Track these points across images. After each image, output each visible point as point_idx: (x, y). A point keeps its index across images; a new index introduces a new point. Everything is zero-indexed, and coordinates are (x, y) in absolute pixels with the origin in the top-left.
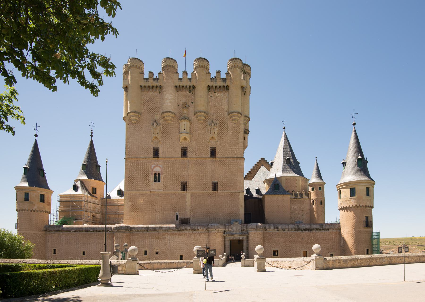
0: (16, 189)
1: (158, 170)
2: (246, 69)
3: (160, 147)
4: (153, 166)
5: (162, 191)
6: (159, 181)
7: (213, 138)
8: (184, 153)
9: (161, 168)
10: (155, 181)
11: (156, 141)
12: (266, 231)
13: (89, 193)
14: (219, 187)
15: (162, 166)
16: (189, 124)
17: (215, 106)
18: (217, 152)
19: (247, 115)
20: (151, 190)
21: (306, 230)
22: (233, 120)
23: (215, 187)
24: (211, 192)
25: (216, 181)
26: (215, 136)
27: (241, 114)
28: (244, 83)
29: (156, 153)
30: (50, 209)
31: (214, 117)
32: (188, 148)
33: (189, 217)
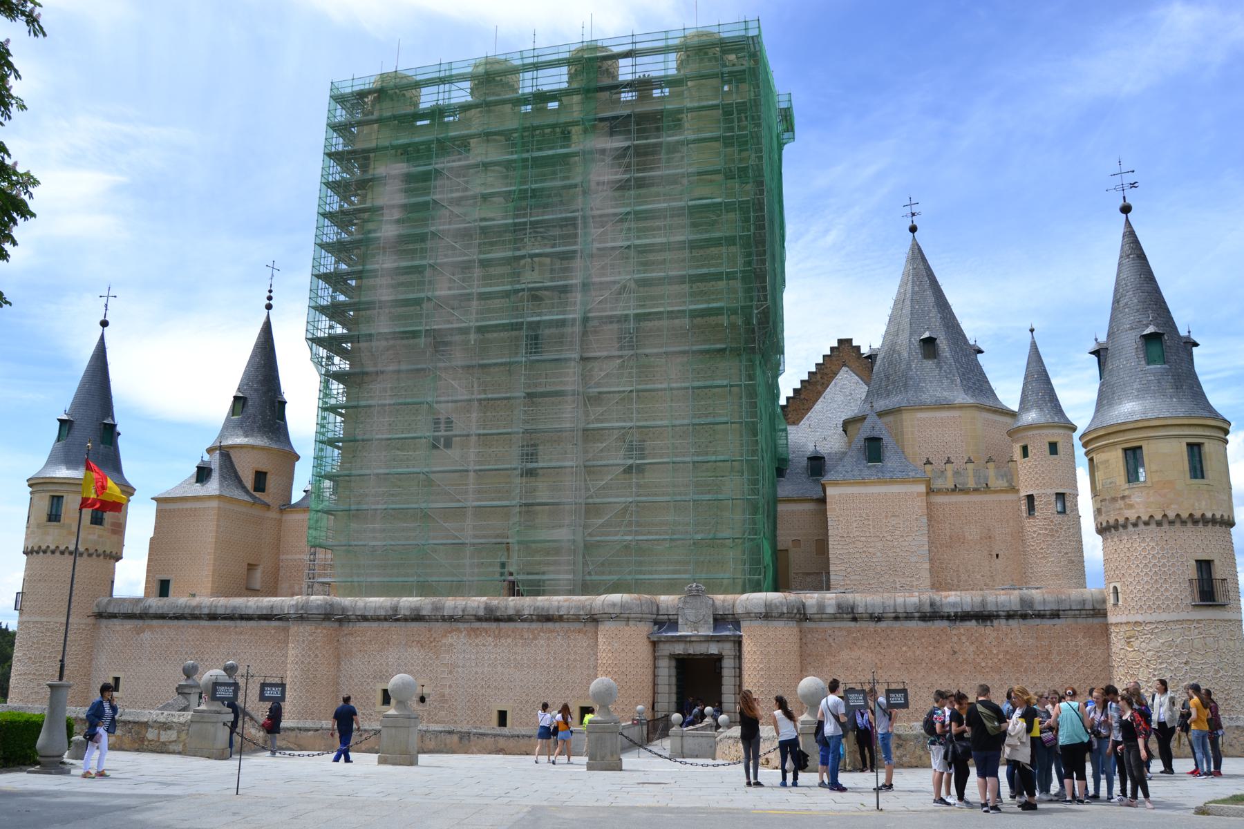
0: (30, 486)
13: (247, 492)
21: (964, 617)
30: (121, 544)
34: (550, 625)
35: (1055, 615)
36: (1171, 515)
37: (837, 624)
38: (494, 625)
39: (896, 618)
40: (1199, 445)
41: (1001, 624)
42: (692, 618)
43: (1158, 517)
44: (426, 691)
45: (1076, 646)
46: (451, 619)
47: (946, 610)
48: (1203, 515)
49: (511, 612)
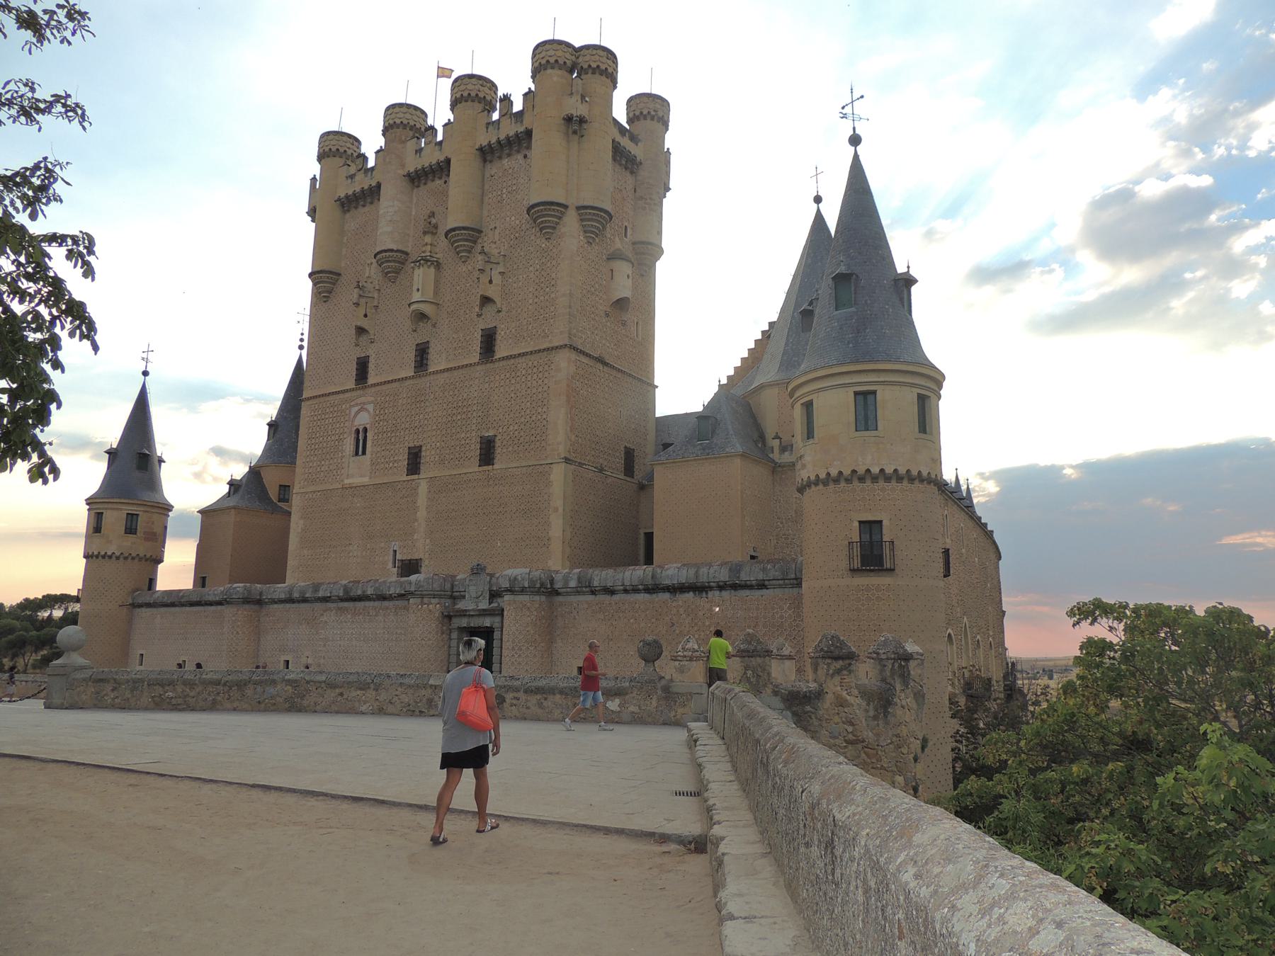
1: (363, 419)
3: (371, 352)
4: (355, 409)
5: (366, 480)
6: (364, 453)
7: (486, 300)
10: (357, 454)
11: (364, 338)
12: (560, 598)
14: (498, 451)
15: (370, 407)
16: (432, 270)
18: (498, 337)
20: (346, 481)
22: (541, 230)
23: (487, 453)
24: (477, 469)
25: (491, 434)
26: (489, 294)
27: (566, 207)
31: (497, 231)
32: (431, 344)
33: (421, 556)
34: (386, 603)
35: (762, 585)
36: (834, 473)
37: (581, 598)
38: (351, 604)
39: (626, 591)
40: (874, 393)
41: (714, 595)
42: (474, 595)
43: (823, 476)
44: (310, 661)
45: (782, 617)
46: (325, 600)
47: (667, 582)
48: (868, 471)
49: (359, 592)
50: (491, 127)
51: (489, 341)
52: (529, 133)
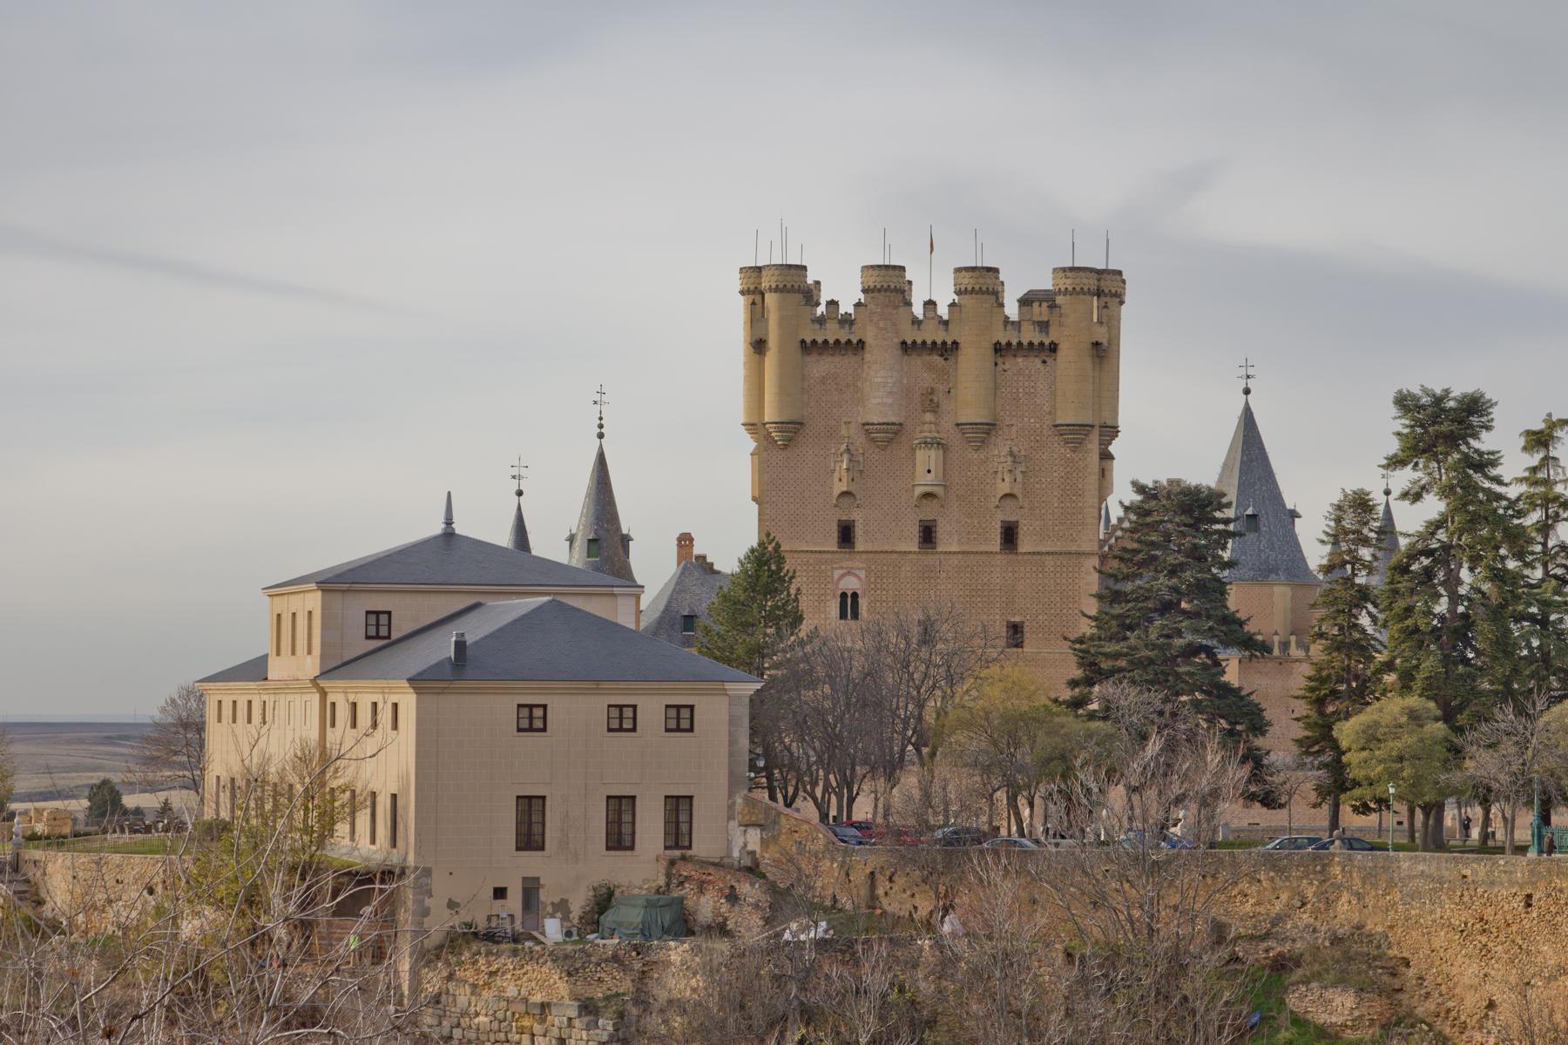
1: (851, 584)
2: (1109, 284)
3: (857, 516)
4: (837, 574)
8: (928, 535)
9: (859, 578)
11: (846, 501)
15: (862, 574)
17: (1017, 399)
18: (1021, 532)
19: (1109, 423)
25: (1017, 619)
26: (1016, 492)
28: (1101, 334)
29: (846, 535)
31: (1014, 429)
50: (1009, 327)
51: (1010, 535)
52: (1054, 348)
